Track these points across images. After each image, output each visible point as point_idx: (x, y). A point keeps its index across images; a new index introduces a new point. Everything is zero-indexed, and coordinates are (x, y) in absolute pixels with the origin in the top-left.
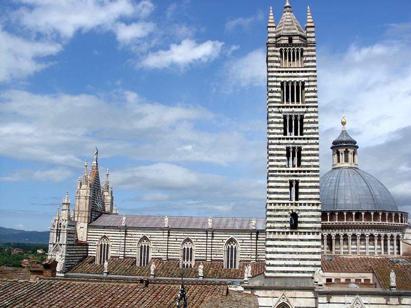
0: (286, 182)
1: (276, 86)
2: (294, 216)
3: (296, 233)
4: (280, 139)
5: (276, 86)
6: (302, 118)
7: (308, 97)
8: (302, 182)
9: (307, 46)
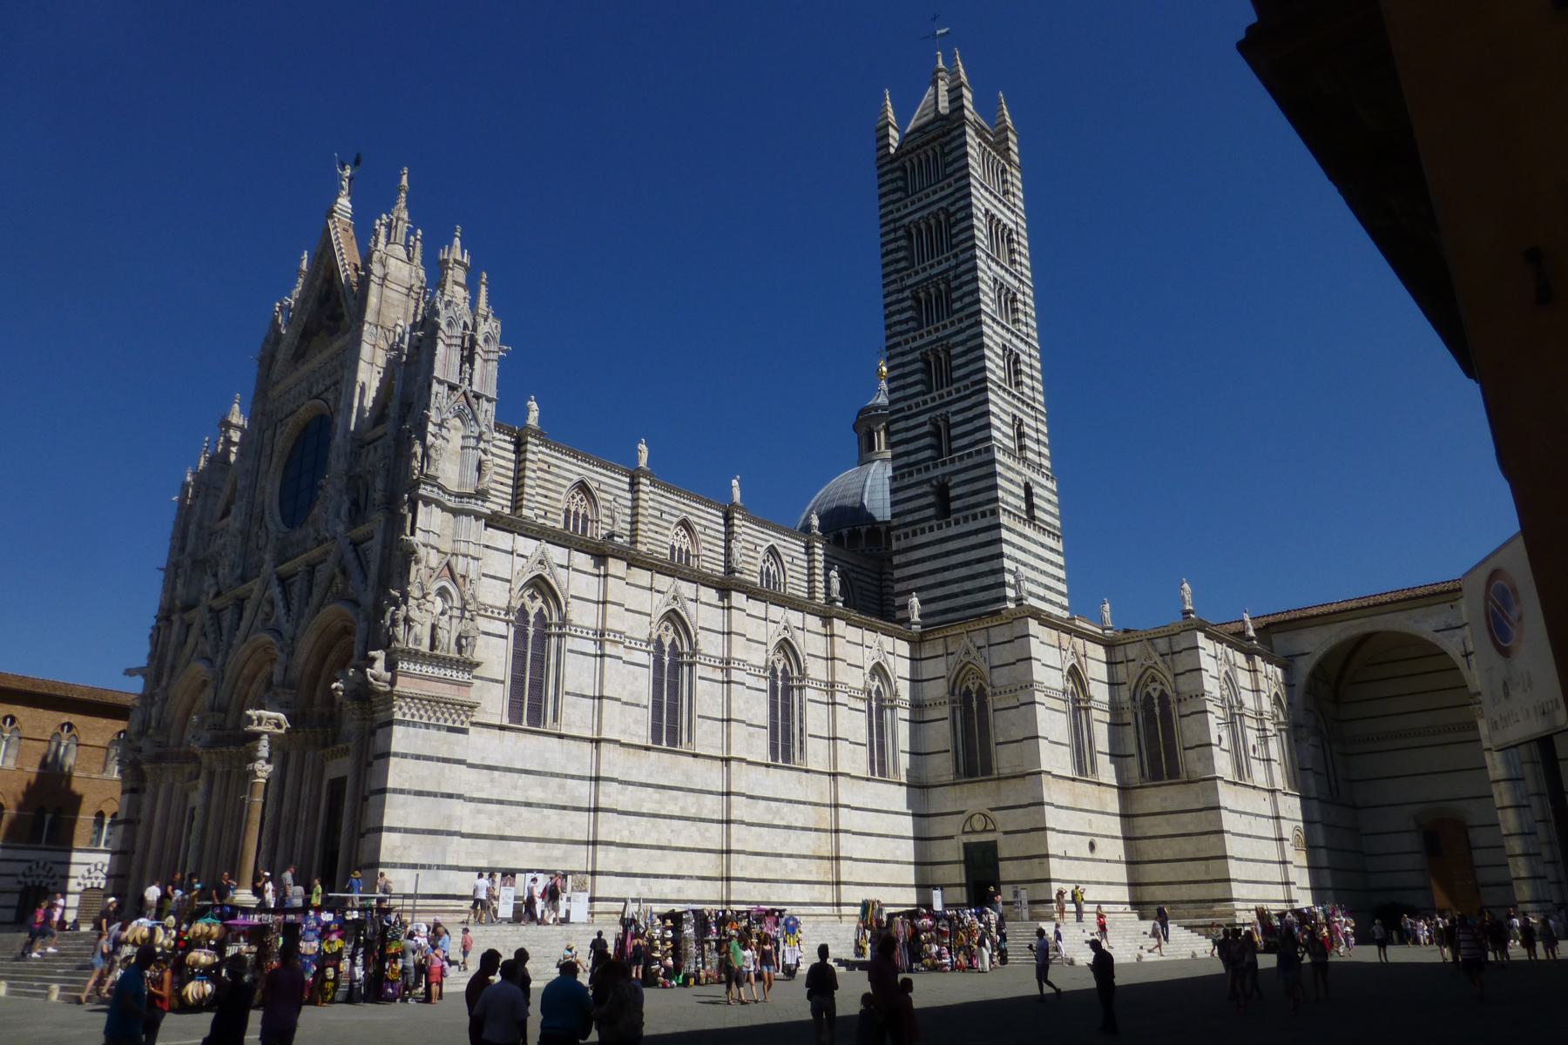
0: (924, 424)
1: (895, 240)
2: (942, 492)
3: (949, 524)
4: (907, 342)
5: (895, 240)
6: (948, 283)
7: (956, 235)
8: (955, 413)
9: (949, 132)
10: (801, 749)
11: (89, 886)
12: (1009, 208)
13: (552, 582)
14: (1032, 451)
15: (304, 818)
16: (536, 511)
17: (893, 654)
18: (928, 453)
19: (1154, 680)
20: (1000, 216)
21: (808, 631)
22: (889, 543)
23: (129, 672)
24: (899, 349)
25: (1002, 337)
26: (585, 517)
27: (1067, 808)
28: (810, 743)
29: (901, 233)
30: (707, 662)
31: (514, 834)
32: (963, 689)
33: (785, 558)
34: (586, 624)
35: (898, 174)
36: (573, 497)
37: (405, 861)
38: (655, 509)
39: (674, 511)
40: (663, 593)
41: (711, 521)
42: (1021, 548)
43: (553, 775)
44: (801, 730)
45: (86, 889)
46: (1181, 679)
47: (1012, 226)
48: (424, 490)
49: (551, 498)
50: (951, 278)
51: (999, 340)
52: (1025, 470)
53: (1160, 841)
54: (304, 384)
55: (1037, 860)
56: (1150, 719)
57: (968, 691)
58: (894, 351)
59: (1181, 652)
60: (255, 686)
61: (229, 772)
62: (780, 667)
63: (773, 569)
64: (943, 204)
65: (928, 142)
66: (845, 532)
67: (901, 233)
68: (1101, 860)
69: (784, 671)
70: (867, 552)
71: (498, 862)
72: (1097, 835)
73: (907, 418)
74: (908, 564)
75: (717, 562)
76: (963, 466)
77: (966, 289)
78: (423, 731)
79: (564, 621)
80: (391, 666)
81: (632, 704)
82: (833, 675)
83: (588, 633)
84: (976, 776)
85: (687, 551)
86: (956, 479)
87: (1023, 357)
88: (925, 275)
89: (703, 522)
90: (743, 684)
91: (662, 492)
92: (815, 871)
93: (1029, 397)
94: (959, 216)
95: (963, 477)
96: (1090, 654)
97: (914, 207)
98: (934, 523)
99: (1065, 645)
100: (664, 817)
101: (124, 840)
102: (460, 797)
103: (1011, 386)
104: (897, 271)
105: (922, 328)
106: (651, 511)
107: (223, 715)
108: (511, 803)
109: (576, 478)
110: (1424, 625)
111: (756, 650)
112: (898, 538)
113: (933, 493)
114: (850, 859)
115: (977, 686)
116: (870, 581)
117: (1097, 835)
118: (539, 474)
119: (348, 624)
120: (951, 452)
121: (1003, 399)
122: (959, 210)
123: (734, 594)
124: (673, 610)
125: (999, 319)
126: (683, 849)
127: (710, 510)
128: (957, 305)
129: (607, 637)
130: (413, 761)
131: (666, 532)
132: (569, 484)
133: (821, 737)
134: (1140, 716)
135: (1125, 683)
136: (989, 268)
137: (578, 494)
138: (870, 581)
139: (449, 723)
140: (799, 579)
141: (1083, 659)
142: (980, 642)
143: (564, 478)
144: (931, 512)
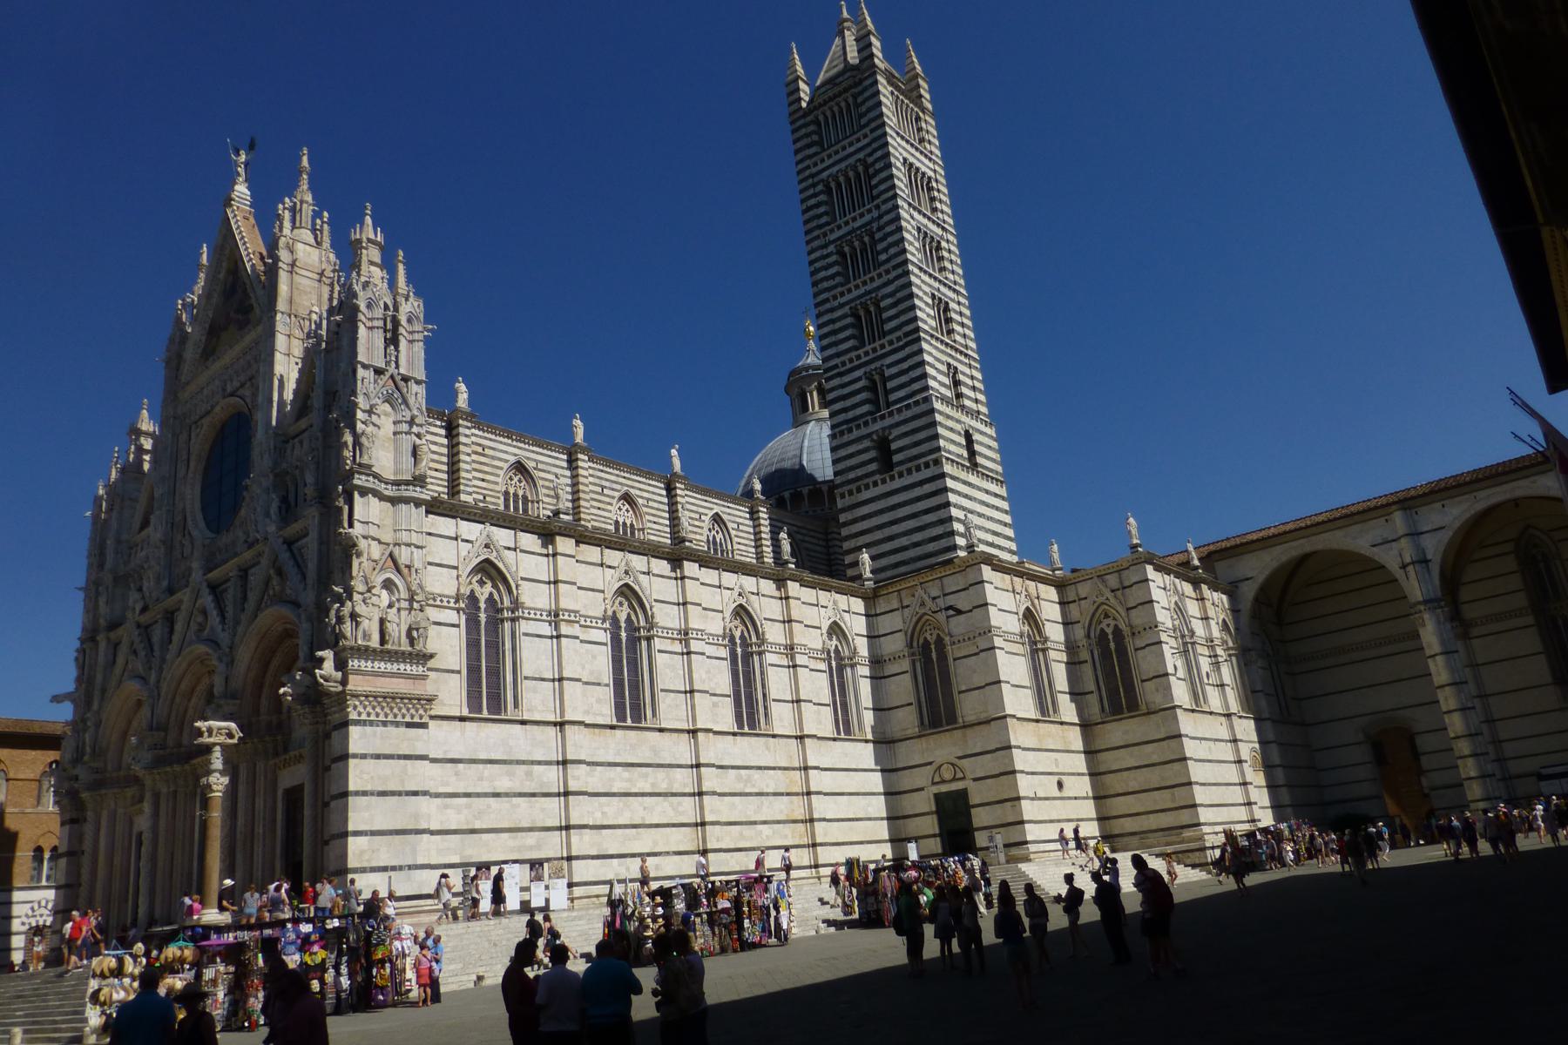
0: (859, 379)
1: (815, 195)
2: (883, 447)
3: (892, 478)
4: (835, 298)
6: (872, 235)
7: (876, 186)
8: (889, 366)
9: (861, 81)
10: (766, 715)
11: (34, 924)
12: (926, 156)
13: (500, 565)
14: (969, 398)
15: (261, 831)
16: (475, 496)
17: (848, 612)
18: (866, 408)
19: (1107, 616)
20: (918, 164)
21: (763, 595)
22: (833, 500)
23: (56, 699)
24: (828, 306)
25: (930, 286)
26: (525, 498)
27: (1034, 750)
28: (775, 708)
29: (820, 187)
30: (665, 635)
31: (484, 827)
32: (921, 641)
33: (730, 525)
34: (540, 606)
35: (812, 128)
36: (511, 479)
37: (374, 864)
38: (595, 484)
39: (615, 486)
40: (614, 568)
41: (653, 493)
42: (966, 496)
43: (519, 762)
44: (764, 695)
45: (31, 928)
46: (1133, 613)
47: (931, 174)
48: (359, 480)
49: (488, 481)
50: (874, 229)
51: (927, 289)
52: (964, 418)
53: (1125, 774)
54: (217, 382)
55: (1009, 804)
56: (1106, 655)
57: (927, 644)
58: (822, 309)
59: (1131, 586)
60: (194, 700)
61: (175, 792)
62: (737, 634)
63: (719, 537)
64: (861, 155)
65: (840, 94)
66: (787, 495)
67: (820, 187)
68: (1069, 798)
69: (742, 637)
70: (811, 513)
71: (471, 857)
72: (1064, 774)
73: (841, 375)
74: (855, 521)
75: (663, 534)
76: (902, 418)
77: (890, 240)
78: (381, 729)
79: (516, 605)
80: (341, 665)
81: (594, 684)
82: (791, 638)
83: (541, 615)
84: (942, 726)
85: (632, 525)
86: (895, 432)
87: (952, 305)
88: (849, 228)
89: (645, 495)
90: (703, 654)
91: (601, 467)
92: (790, 836)
93: (961, 345)
94: (878, 166)
95: (904, 429)
96: (1042, 595)
97: (831, 161)
98: (877, 477)
99: (1018, 588)
100: (636, 795)
101: (68, 873)
102: (425, 793)
103: (942, 335)
104: (820, 227)
105: (850, 282)
106: (591, 487)
107: (163, 734)
108: (478, 795)
109: (512, 459)
110: (1360, 540)
111: (713, 618)
112: (843, 496)
113: (874, 448)
114: (824, 820)
115: (934, 637)
116: (816, 541)
117: (1064, 774)
118: (474, 457)
119: (288, 626)
120: (888, 405)
121: (936, 348)
122: (876, 161)
123: (686, 564)
124: (626, 585)
125: (925, 267)
126: (657, 826)
127: (651, 482)
128: (883, 257)
129: (561, 617)
130: (373, 761)
131: (609, 507)
132: (506, 466)
133: (784, 701)
134: (1096, 653)
135: (1079, 622)
136: (912, 217)
137: (516, 475)
138: (816, 541)
139: (408, 719)
140: (746, 545)
141: (1036, 601)
142: (935, 593)
143: (500, 460)
144: (873, 467)
